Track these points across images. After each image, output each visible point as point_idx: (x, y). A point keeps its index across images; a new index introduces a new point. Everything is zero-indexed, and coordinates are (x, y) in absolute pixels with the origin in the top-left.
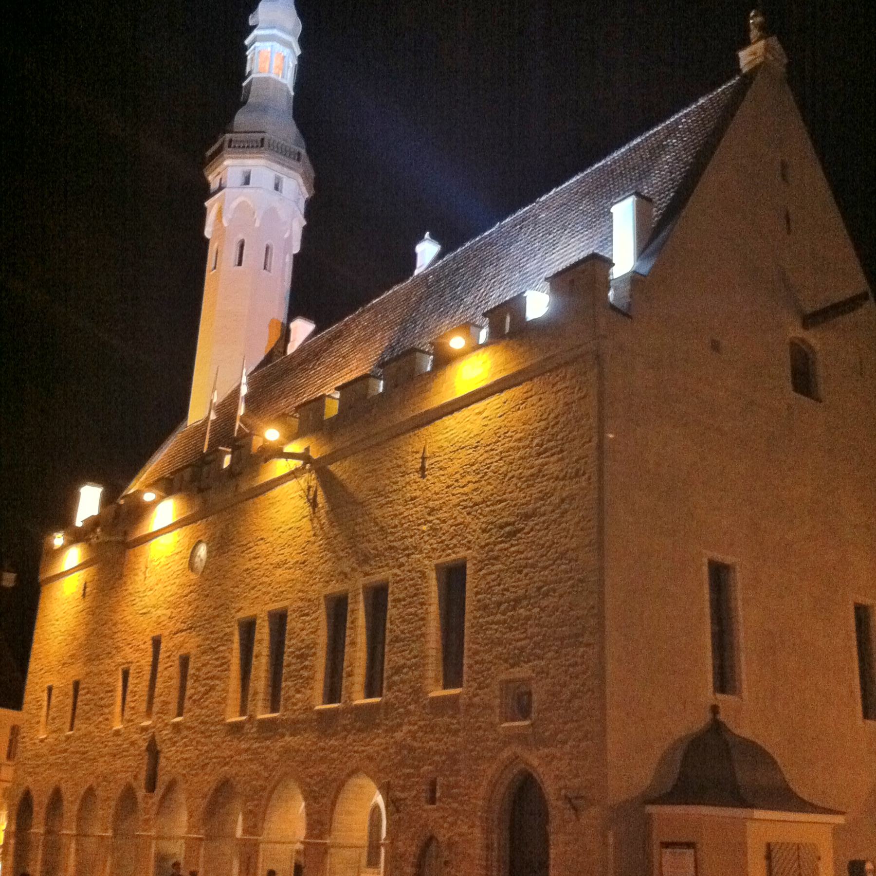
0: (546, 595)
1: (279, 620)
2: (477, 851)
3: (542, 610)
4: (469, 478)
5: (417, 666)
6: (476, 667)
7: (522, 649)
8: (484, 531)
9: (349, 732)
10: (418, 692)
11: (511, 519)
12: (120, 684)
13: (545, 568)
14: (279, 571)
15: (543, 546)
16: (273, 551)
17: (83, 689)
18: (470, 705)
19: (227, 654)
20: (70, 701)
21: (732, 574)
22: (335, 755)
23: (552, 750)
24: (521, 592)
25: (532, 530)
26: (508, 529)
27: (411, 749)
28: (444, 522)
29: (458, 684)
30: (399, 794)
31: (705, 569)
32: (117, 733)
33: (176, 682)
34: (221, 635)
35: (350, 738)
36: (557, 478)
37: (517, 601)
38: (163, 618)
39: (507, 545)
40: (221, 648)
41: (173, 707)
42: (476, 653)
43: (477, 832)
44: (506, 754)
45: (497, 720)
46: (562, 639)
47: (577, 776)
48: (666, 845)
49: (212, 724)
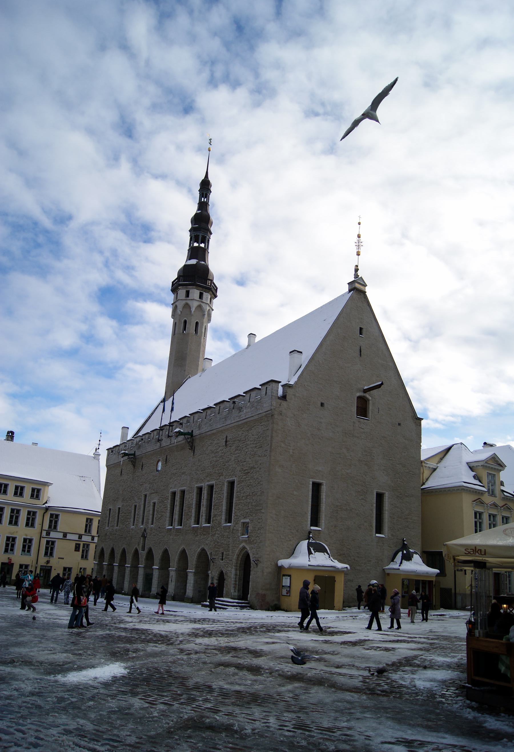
1: (183, 492)
2: (233, 576)
4: (237, 452)
6: (236, 517)
7: (247, 513)
8: (240, 471)
10: (220, 523)
11: (247, 468)
12: (133, 511)
18: (233, 529)
20: (117, 515)
21: (322, 487)
23: (252, 545)
24: (248, 494)
26: (246, 471)
27: (218, 542)
29: (231, 523)
30: (214, 557)
31: (311, 486)
32: (132, 529)
33: (151, 512)
36: (259, 456)
37: (247, 496)
39: (245, 477)
41: (150, 521)
43: (233, 571)
44: (241, 546)
45: (240, 535)
46: (257, 510)
47: (258, 554)
48: (284, 575)
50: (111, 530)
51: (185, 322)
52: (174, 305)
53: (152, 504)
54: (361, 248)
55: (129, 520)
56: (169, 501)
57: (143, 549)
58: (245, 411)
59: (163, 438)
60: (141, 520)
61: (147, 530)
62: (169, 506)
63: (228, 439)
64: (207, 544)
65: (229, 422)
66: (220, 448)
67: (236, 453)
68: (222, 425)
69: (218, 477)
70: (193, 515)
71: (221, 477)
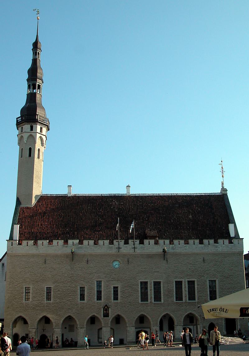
0: (235, 288)
3: (235, 290)
4: (215, 266)
5: (206, 296)
9: (187, 306)
12: (79, 291)
13: (235, 284)
14: (155, 273)
15: (234, 281)
16: (152, 268)
17: (54, 290)
19: (137, 288)
22: (183, 310)
24: (230, 287)
25: (231, 278)
28: (210, 273)
34: (133, 284)
35: (188, 307)
38: (102, 276)
40: (133, 287)
42: (220, 295)
49: (134, 303)
50: (36, 303)
51: (39, 150)
52: (29, 134)
53: (112, 288)
54: (224, 173)
55: (73, 297)
56: (140, 287)
57: (106, 315)
58: (221, 248)
59: (120, 247)
60: (96, 297)
61: (110, 304)
62: (140, 290)
63: (204, 259)
64: (195, 311)
65: (207, 251)
66: (198, 263)
67: (214, 267)
68: (199, 251)
69: (199, 278)
70: (175, 296)
71: (203, 278)
